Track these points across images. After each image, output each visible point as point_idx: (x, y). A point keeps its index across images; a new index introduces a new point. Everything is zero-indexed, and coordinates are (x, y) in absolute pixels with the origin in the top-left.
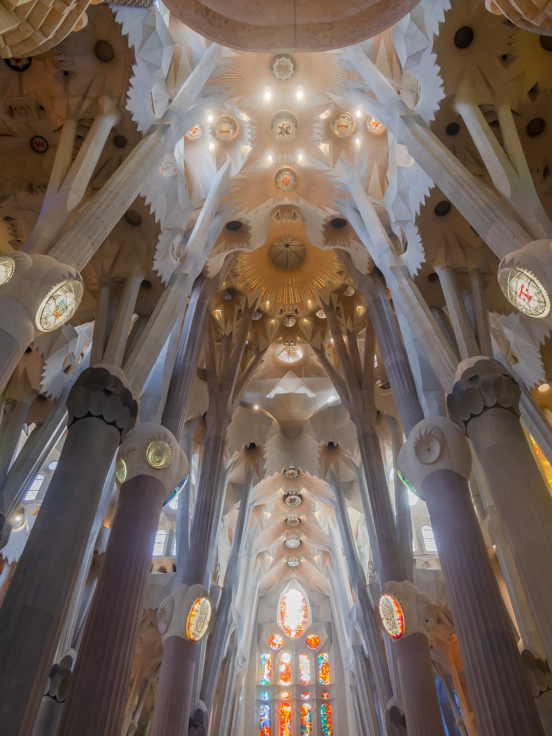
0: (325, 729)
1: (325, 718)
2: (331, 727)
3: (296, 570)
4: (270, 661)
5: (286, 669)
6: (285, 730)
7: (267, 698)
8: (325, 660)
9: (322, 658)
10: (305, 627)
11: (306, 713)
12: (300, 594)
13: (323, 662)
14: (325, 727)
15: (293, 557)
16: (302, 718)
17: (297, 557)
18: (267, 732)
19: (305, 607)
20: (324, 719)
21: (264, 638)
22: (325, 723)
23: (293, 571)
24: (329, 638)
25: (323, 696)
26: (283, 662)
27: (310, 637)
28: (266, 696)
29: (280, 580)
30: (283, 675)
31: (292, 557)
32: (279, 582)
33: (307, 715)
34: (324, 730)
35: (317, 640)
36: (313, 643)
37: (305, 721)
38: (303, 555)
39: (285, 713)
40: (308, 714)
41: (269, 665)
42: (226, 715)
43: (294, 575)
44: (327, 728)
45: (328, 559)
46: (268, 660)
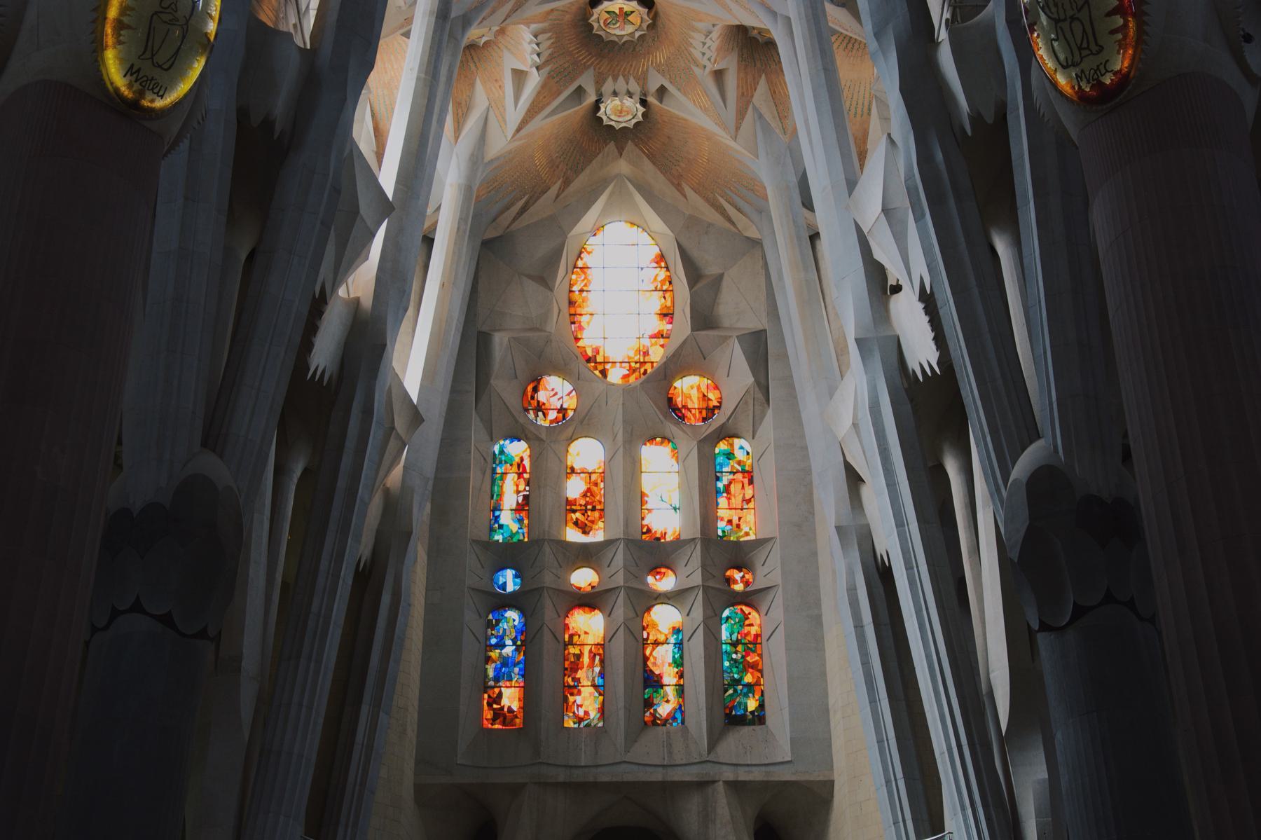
0: (735, 691)
1: (736, 653)
2: (758, 683)
3: (630, 146)
4: (527, 463)
5: (589, 490)
6: (579, 693)
7: (510, 588)
8: (739, 463)
9: (729, 455)
10: (662, 350)
11: (662, 638)
12: (645, 238)
13: (732, 467)
14: (738, 682)
15: (621, 79)
16: (648, 652)
17: (637, 79)
18: (512, 699)
19: (663, 282)
20: (734, 656)
21: (504, 388)
22: (735, 670)
23: (620, 151)
24: (757, 382)
25: (729, 581)
26: (577, 467)
27: (688, 387)
28: (509, 580)
29: (567, 183)
30: (574, 511)
31: (615, 79)
32: (561, 190)
33: (666, 642)
34: (731, 691)
35: (711, 396)
36: (695, 403)
37: (659, 662)
38: (658, 71)
39: (583, 636)
40: (672, 640)
41: (520, 476)
42: (337, 576)
43: (623, 167)
44: (745, 686)
45: (762, 86)
46: (517, 459)
